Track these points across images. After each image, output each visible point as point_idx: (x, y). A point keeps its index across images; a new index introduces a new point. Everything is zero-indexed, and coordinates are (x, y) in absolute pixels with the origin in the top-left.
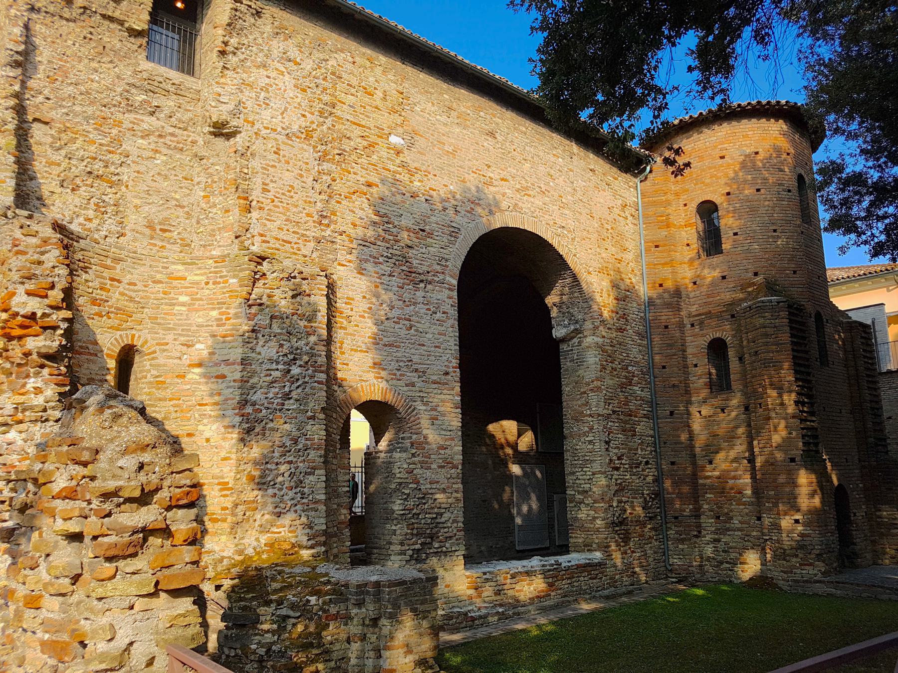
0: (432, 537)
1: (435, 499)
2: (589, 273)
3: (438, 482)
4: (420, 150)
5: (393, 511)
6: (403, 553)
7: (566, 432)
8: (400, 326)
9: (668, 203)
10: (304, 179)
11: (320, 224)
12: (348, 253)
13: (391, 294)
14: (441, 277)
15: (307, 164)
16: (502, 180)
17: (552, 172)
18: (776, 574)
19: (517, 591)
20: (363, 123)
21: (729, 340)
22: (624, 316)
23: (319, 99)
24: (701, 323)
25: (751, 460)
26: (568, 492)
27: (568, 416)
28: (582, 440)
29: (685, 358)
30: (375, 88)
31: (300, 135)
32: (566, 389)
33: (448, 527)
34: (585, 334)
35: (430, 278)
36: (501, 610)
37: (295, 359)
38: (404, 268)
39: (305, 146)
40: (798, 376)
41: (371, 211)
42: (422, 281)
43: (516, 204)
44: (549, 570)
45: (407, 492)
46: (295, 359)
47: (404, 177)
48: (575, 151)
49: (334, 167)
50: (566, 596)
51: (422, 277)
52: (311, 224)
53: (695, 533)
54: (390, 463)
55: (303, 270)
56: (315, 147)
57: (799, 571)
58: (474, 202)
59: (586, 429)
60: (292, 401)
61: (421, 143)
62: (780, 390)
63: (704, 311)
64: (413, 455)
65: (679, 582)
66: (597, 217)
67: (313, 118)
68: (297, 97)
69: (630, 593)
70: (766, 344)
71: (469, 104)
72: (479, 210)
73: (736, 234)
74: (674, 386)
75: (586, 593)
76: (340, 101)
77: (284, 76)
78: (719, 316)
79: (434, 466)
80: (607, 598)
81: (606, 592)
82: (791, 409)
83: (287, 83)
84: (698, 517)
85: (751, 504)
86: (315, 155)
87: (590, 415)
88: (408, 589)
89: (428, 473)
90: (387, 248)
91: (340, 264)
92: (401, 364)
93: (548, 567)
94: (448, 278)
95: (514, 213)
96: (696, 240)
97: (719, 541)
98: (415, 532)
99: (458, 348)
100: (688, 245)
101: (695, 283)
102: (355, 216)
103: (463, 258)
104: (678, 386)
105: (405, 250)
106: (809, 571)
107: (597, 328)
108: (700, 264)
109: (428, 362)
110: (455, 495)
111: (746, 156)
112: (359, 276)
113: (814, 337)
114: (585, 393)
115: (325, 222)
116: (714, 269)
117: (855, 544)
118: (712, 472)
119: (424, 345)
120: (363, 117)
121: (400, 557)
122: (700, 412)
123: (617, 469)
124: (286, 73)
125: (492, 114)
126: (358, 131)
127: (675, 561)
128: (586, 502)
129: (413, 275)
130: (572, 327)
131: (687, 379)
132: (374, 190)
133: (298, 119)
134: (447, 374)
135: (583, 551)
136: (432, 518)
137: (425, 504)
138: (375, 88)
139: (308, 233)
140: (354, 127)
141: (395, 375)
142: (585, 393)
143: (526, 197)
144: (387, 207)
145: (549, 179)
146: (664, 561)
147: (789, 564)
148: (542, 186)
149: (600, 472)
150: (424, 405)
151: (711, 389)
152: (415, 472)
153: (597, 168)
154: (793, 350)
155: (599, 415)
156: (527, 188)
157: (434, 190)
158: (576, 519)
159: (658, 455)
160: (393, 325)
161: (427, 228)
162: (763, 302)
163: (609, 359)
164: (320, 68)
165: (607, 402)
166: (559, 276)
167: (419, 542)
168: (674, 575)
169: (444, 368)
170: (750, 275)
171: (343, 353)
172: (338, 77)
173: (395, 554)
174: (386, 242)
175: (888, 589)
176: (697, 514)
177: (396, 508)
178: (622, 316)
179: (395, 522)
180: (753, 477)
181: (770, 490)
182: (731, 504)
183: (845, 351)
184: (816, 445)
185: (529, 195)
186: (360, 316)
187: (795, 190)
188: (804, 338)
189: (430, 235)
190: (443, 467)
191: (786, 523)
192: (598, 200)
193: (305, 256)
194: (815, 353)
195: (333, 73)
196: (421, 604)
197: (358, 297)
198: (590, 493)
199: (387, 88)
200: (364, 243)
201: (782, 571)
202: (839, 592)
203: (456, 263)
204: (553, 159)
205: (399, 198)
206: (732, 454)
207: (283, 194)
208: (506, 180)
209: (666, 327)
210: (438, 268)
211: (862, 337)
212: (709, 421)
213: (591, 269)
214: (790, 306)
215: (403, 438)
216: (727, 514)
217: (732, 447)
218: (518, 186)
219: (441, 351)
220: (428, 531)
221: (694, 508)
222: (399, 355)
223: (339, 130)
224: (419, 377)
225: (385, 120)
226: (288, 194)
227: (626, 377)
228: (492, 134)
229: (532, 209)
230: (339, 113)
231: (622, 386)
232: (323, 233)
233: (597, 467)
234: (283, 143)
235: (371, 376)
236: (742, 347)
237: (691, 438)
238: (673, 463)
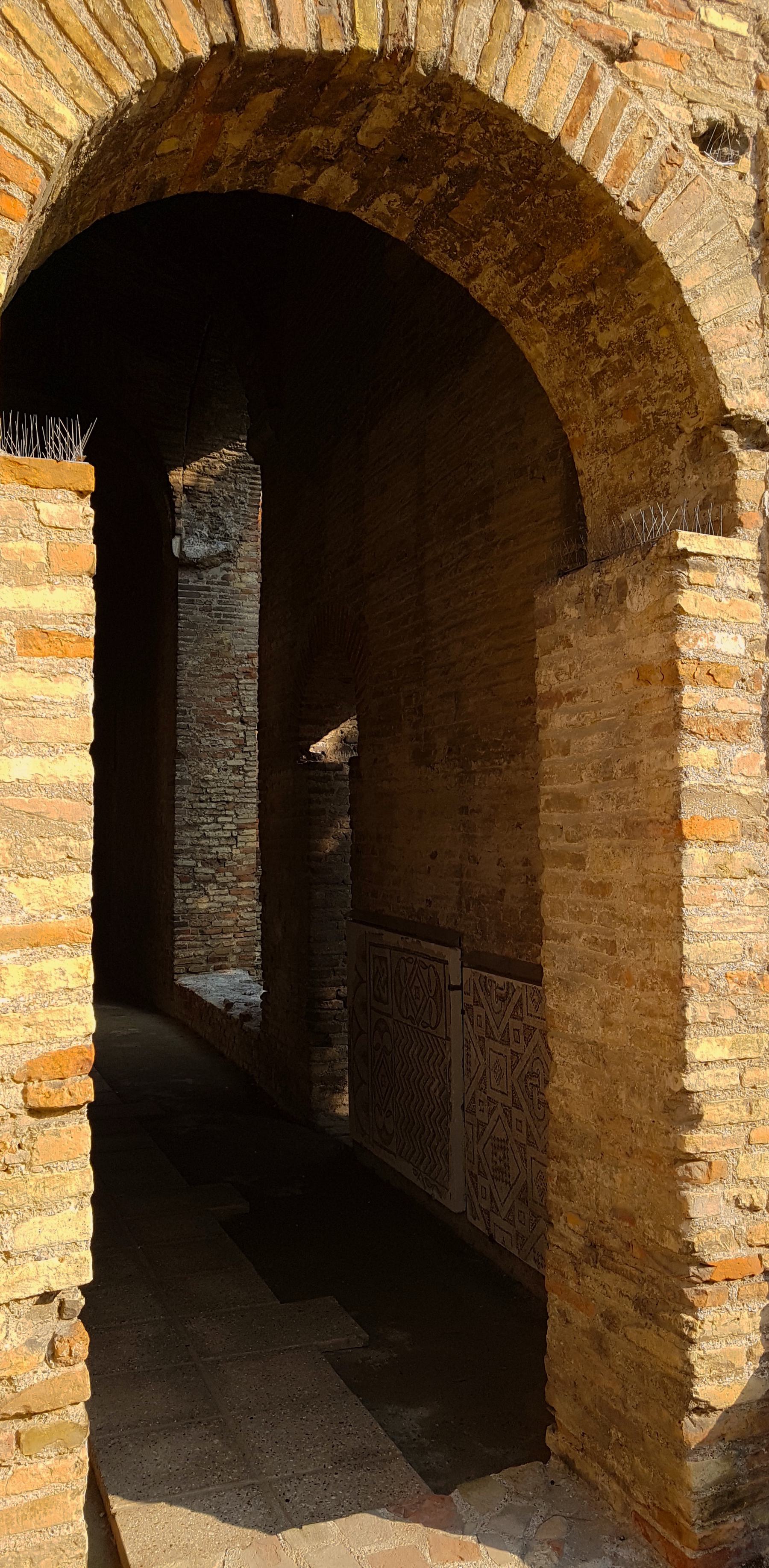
28: (220, 763)
32: (189, 663)
59: (230, 744)
114: (232, 675)
130: (222, 547)
142: (232, 675)
158: (191, 913)
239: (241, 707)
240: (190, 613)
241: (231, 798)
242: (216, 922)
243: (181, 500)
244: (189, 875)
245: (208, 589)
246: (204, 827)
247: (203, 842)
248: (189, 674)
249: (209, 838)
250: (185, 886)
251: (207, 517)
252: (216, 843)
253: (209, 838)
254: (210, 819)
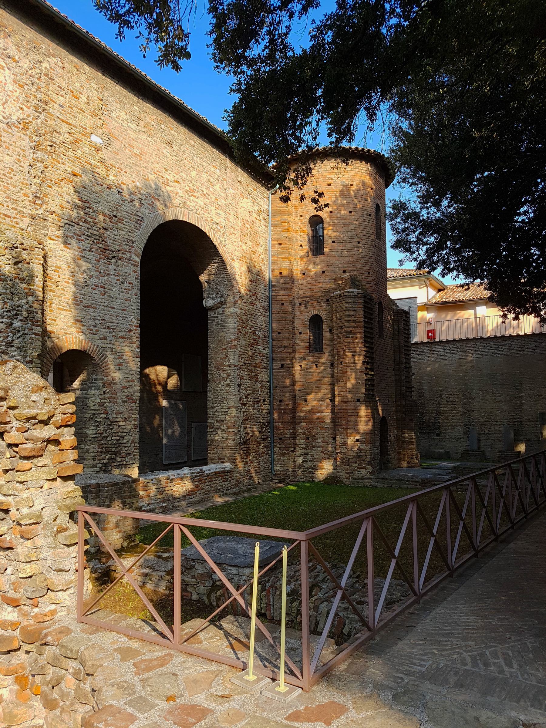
0: (116, 454)
1: (119, 426)
2: (234, 260)
3: (121, 413)
4: (115, 150)
5: (87, 435)
6: (94, 466)
7: (209, 377)
8: (96, 292)
9: (290, 214)
10: (22, 164)
11: (35, 203)
12: (57, 230)
13: (90, 266)
14: (129, 256)
15: (24, 151)
16: (176, 182)
17: (212, 180)
18: (342, 475)
19: (174, 491)
20: (70, 121)
21: (324, 316)
22: (255, 294)
23: (34, 96)
24: (306, 303)
25: (332, 400)
26: (209, 421)
27: (212, 365)
28: (222, 383)
29: (293, 327)
30: (81, 93)
31: (18, 125)
32: (211, 345)
33: (128, 447)
34: (228, 305)
35: (120, 255)
36: (164, 505)
37: (17, 315)
38: (101, 246)
39: (23, 136)
40: (366, 345)
41: (75, 197)
42: (114, 257)
43: (185, 202)
44: (197, 476)
45: (98, 420)
46: (17, 315)
47: (102, 171)
48: (229, 165)
49: (46, 156)
50: (207, 494)
51: (114, 254)
52: (27, 202)
53: (292, 449)
54: (85, 398)
55: (24, 242)
56: (30, 137)
57: (356, 472)
58: (154, 196)
60: (13, 348)
61: (116, 144)
62: (354, 353)
63: (309, 294)
64: (104, 392)
65: (280, 482)
66: (241, 218)
67: (29, 112)
68: (16, 91)
69: (249, 490)
70: (348, 322)
71: (154, 117)
72: (157, 203)
73: (334, 242)
74: (285, 347)
75: (220, 492)
76: (52, 100)
77: (4, 70)
78: (319, 299)
79: (119, 401)
80: (235, 494)
81: (233, 490)
82: (359, 366)
83: (7, 78)
84: (295, 438)
85: (330, 429)
86: (31, 144)
87: (229, 366)
88: (120, 488)
89: (115, 407)
90: (88, 228)
91: (50, 239)
92: (97, 322)
93: (196, 474)
94: (133, 256)
95: (183, 209)
96: (306, 243)
97: (307, 454)
98: (104, 450)
99: (139, 311)
100: (301, 246)
101: (304, 274)
102: (61, 198)
103: (145, 241)
104: (288, 347)
105: (102, 231)
106: (363, 472)
107: (236, 301)
108: (308, 261)
109: (117, 321)
110: (133, 422)
111: (344, 186)
112: (66, 249)
113: (377, 319)
115: (39, 202)
116: (317, 265)
117: (389, 455)
118: (304, 408)
119: (114, 308)
120: (70, 116)
121: (92, 469)
122: (301, 366)
123: (244, 405)
124: (6, 68)
125: (170, 127)
126: (65, 128)
127: (277, 468)
128: (222, 428)
129: (108, 252)
130: (219, 300)
131: (294, 342)
132: (78, 179)
133: (17, 111)
134: (130, 331)
135: (218, 463)
136: (117, 440)
137: (111, 429)
138: (81, 93)
139: (24, 210)
140: (63, 124)
141: (92, 330)
142: (225, 349)
143: (192, 198)
144: (89, 195)
145: (209, 185)
146: (271, 469)
147: (351, 468)
148: (204, 190)
149: (233, 407)
150: (113, 354)
151: (309, 350)
152: (105, 405)
153: (243, 180)
154: (365, 327)
155: (235, 366)
156: (193, 191)
157: (125, 184)
158: (213, 440)
159: (271, 394)
160: (91, 290)
161: (119, 214)
162: (348, 292)
163: (244, 325)
164: (35, 68)
165: (241, 357)
166: (211, 260)
167: (107, 457)
168: (276, 478)
169: (128, 326)
170: (341, 272)
171: (52, 311)
172: (50, 78)
173: (88, 467)
174: (87, 223)
175: (407, 481)
176: (294, 436)
177: (90, 432)
178: (253, 292)
179: (89, 443)
180: (333, 412)
181: (342, 420)
182: (317, 430)
183: (394, 329)
184: (373, 390)
185: (195, 196)
186: (66, 282)
187: (373, 216)
188: (371, 319)
189: (121, 221)
190: (125, 402)
191: (351, 441)
192: (242, 205)
193: (22, 230)
194: (376, 330)
195: (46, 75)
196: (128, 498)
197: (65, 267)
198: (225, 422)
199: (90, 94)
200: (70, 223)
201: (346, 473)
202: (379, 484)
203: (140, 245)
204: (213, 169)
205: (97, 188)
206: (320, 395)
207: (4, 175)
208: (178, 182)
209: (283, 304)
210: (126, 248)
211: (404, 320)
212: (306, 372)
213: (235, 257)
214: (365, 297)
215: (96, 379)
216: (314, 436)
217: (319, 391)
218: (187, 188)
219: (126, 313)
220: (114, 450)
221: (293, 432)
222: (95, 314)
223: (51, 126)
224: (110, 333)
225: (88, 121)
226: (8, 175)
227: (254, 339)
228: (169, 143)
229: (196, 207)
230: (51, 110)
231: (251, 345)
232: (37, 212)
233: (231, 403)
234: (4, 130)
235: (73, 330)
236: (332, 322)
237: (293, 382)
238: (281, 401)
239: (229, 361)
240: (212, 327)
241: (225, 397)
242: (221, 444)
245: (217, 317)
247: (216, 413)
250: (211, 430)
252: (221, 414)
254: (219, 405)
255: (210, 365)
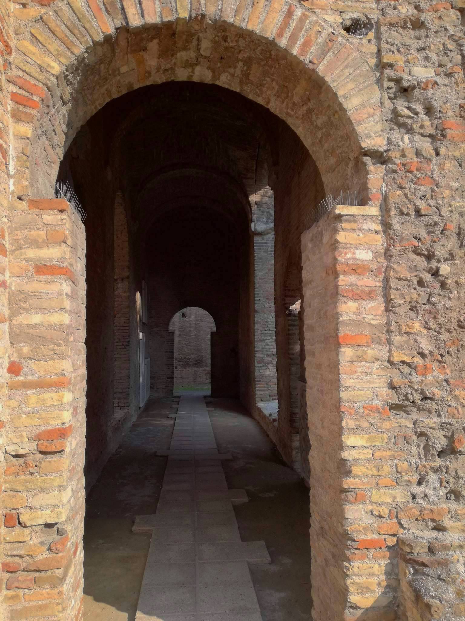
158: (262, 376)
243: (254, 208)
244: (262, 361)
245: (266, 243)
246: (267, 341)
248: (260, 278)
249: (269, 345)
250: (260, 365)
251: (265, 213)
253: (269, 345)
254: (269, 338)
255: (258, 294)
